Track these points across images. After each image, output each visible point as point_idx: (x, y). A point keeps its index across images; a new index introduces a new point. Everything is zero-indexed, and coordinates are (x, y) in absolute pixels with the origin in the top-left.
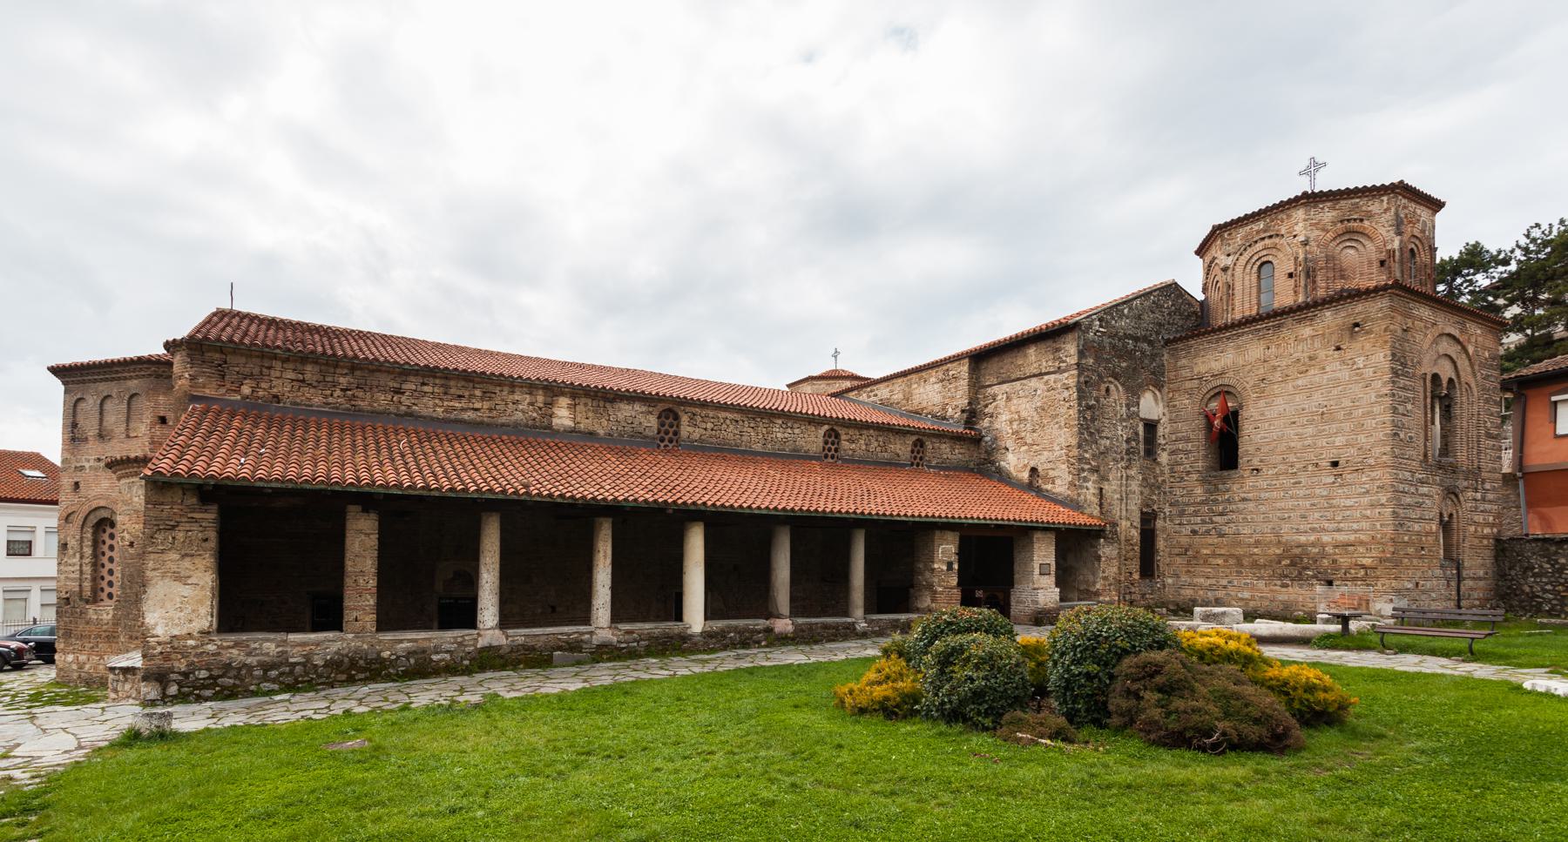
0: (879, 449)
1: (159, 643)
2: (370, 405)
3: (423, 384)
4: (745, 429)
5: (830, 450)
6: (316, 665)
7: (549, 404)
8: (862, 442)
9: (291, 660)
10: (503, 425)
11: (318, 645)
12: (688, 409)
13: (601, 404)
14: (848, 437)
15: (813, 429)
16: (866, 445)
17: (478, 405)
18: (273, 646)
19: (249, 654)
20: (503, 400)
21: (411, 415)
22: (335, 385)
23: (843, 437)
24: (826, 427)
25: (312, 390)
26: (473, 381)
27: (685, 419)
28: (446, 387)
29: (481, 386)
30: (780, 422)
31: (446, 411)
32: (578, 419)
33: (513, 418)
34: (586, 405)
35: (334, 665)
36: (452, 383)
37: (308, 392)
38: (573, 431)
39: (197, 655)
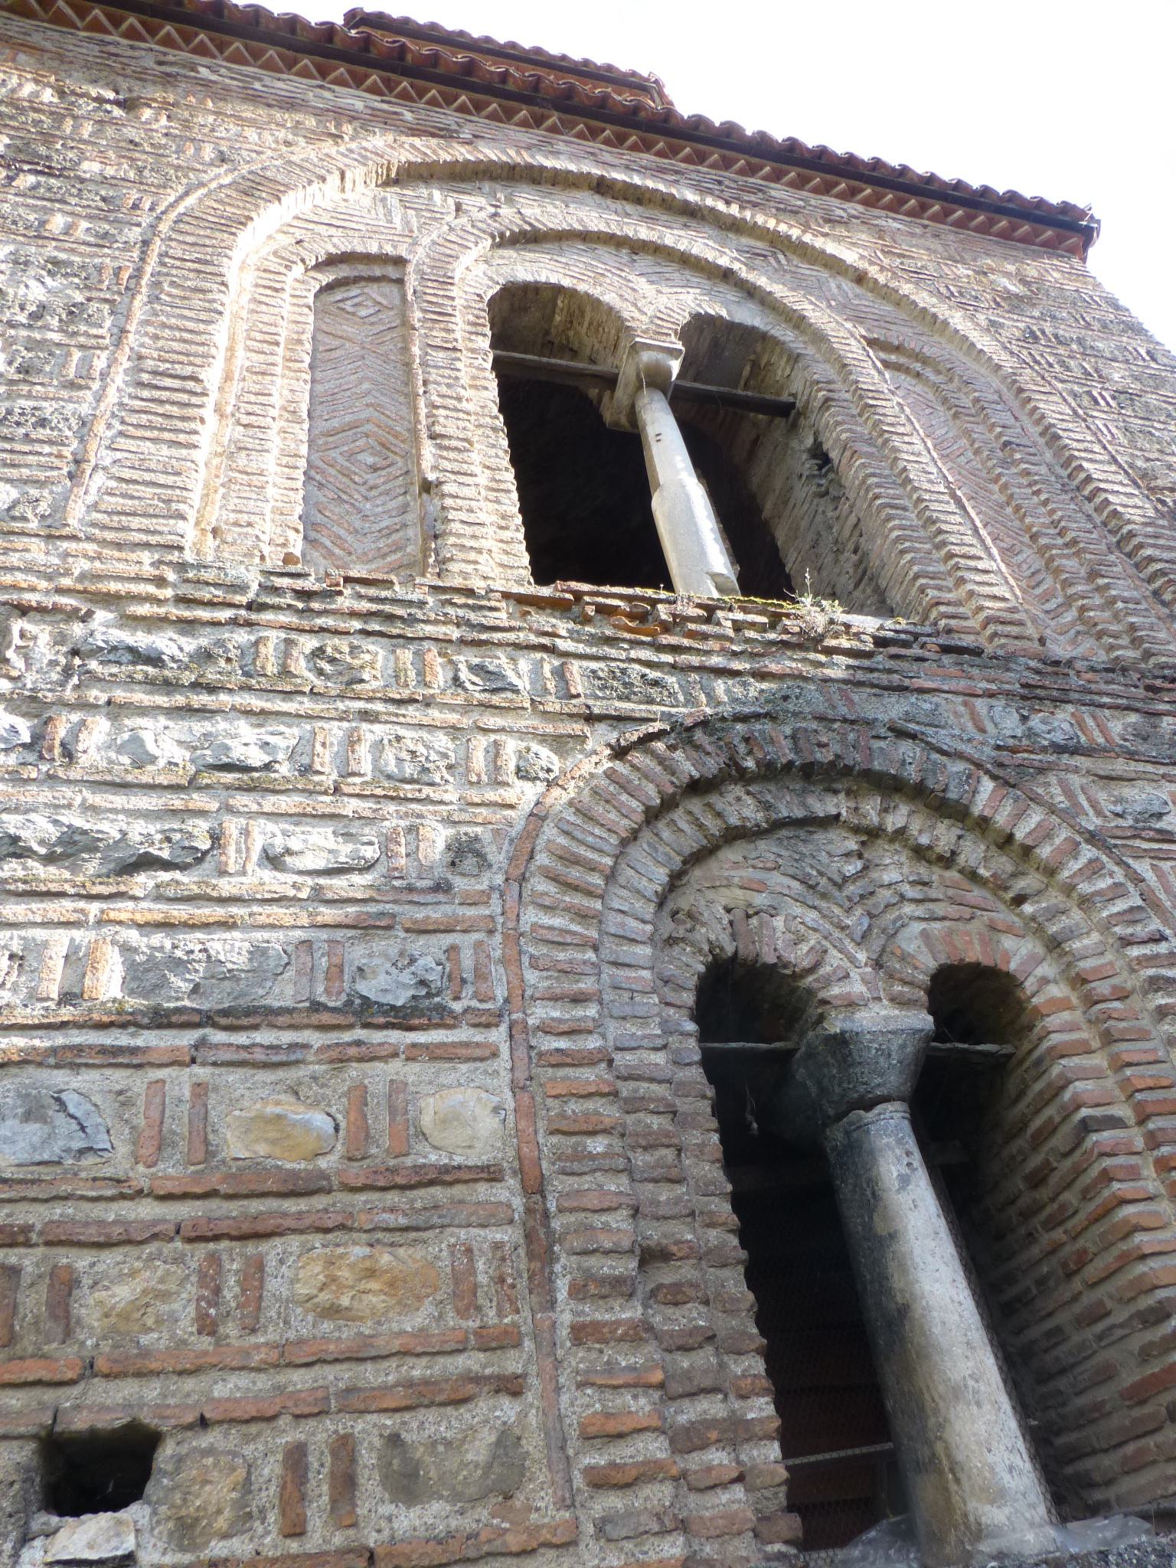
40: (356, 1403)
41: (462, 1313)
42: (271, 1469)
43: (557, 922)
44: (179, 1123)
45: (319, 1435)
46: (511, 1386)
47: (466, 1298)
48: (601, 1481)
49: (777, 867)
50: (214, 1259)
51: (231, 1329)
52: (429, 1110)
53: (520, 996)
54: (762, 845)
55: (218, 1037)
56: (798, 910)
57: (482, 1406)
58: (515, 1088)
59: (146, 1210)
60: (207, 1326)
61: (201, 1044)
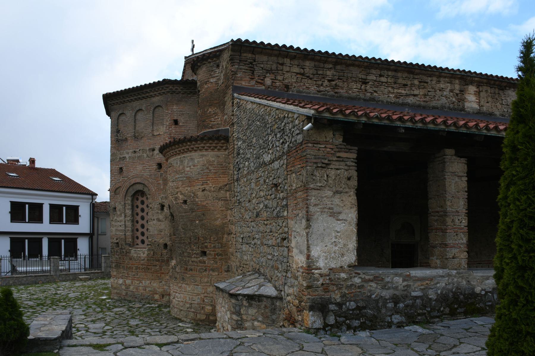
1: (321, 275)
2: (347, 92)
3: (381, 76)
6: (431, 299)
9: (414, 294)
10: (434, 108)
11: (432, 280)
13: (497, 91)
17: (416, 92)
18: (401, 280)
19: (384, 288)
20: (433, 88)
21: (373, 99)
22: (324, 77)
25: (310, 81)
26: (413, 73)
28: (396, 78)
29: (418, 77)
31: (396, 97)
32: (482, 103)
33: (440, 102)
34: (487, 91)
35: (443, 298)
36: (399, 75)
37: (307, 83)
38: (479, 113)
39: (348, 287)
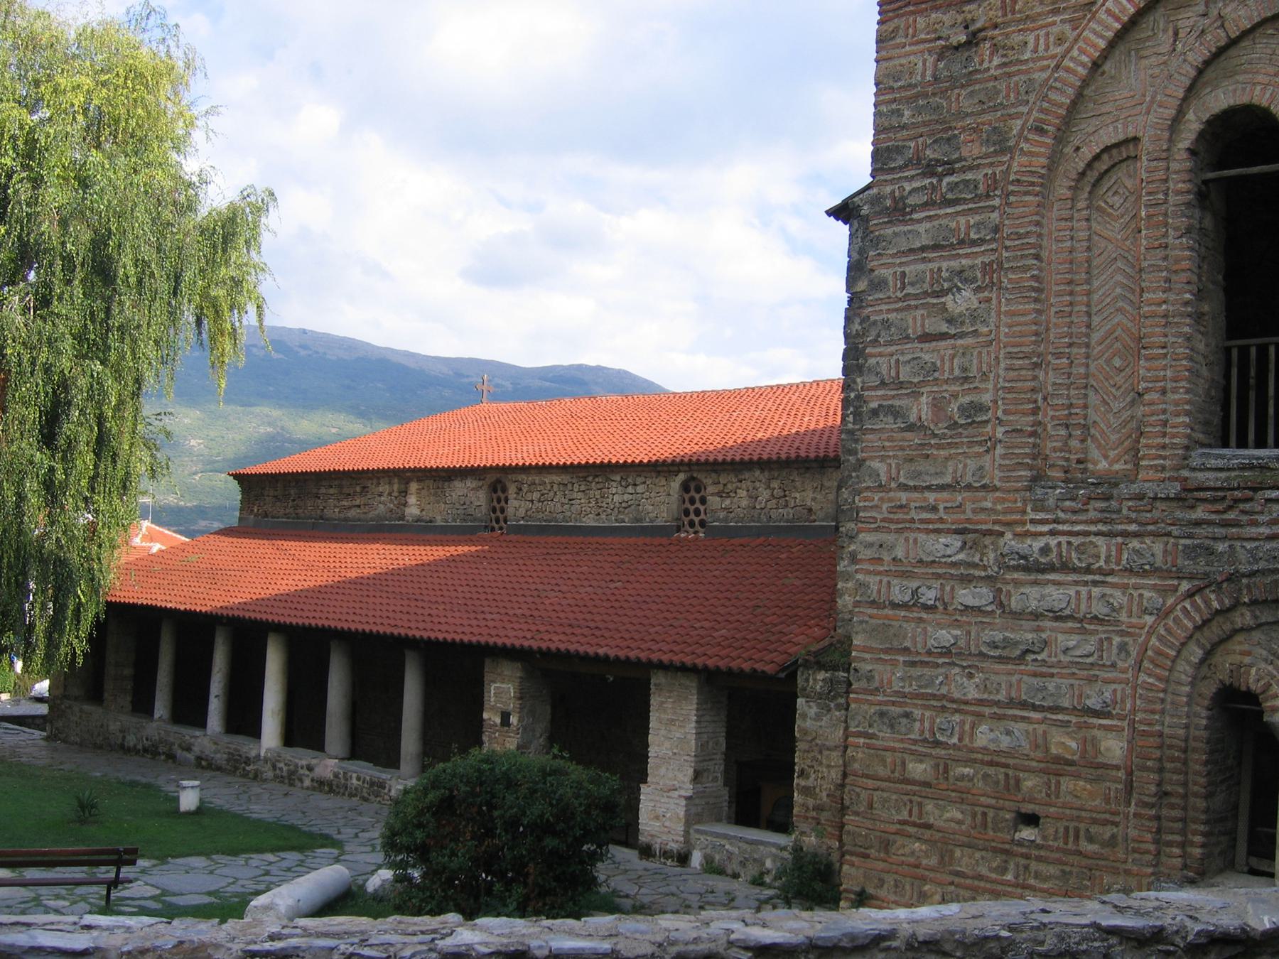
0: (773, 503)
4: (575, 496)
5: (697, 512)
7: (405, 493)
8: (743, 493)
12: (514, 477)
14: (721, 487)
15: (663, 482)
16: (751, 497)
17: (357, 502)
23: (711, 489)
24: (682, 477)
27: (512, 489)
28: (341, 487)
30: (618, 478)
36: (344, 483)
40: (1079, 819)
41: (1106, 804)
42: (1061, 830)
43: (1151, 680)
44: (1040, 741)
45: (1072, 825)
46: (1116, 824)
47: (1107, 800)
48: (1134, 851)
49: (1259, 644)
50: (1049, 779)
51: (1053, 797)
52: (1103, 745)
53: (1134, 710)
54: (1254, 633)
55: (1049, 716)
56: (1263, 665)
57: (1109, 827)
58: (1129, 742)
59: (1034, 764)
60: (1048, 795)
61: (1045, 718)
